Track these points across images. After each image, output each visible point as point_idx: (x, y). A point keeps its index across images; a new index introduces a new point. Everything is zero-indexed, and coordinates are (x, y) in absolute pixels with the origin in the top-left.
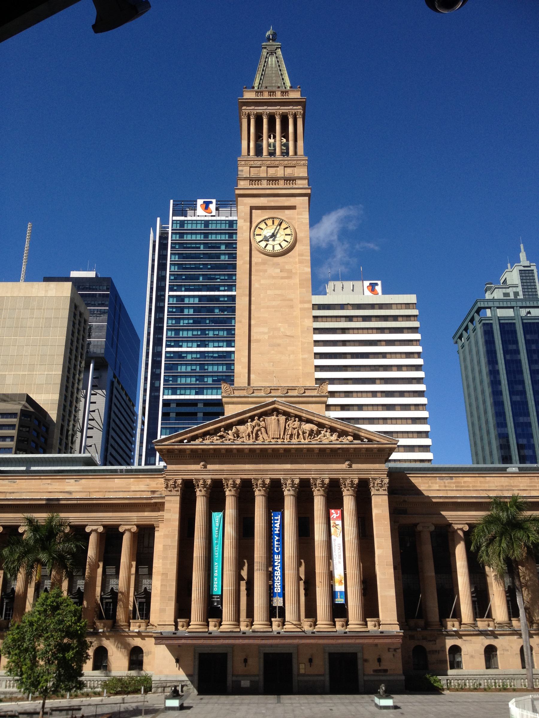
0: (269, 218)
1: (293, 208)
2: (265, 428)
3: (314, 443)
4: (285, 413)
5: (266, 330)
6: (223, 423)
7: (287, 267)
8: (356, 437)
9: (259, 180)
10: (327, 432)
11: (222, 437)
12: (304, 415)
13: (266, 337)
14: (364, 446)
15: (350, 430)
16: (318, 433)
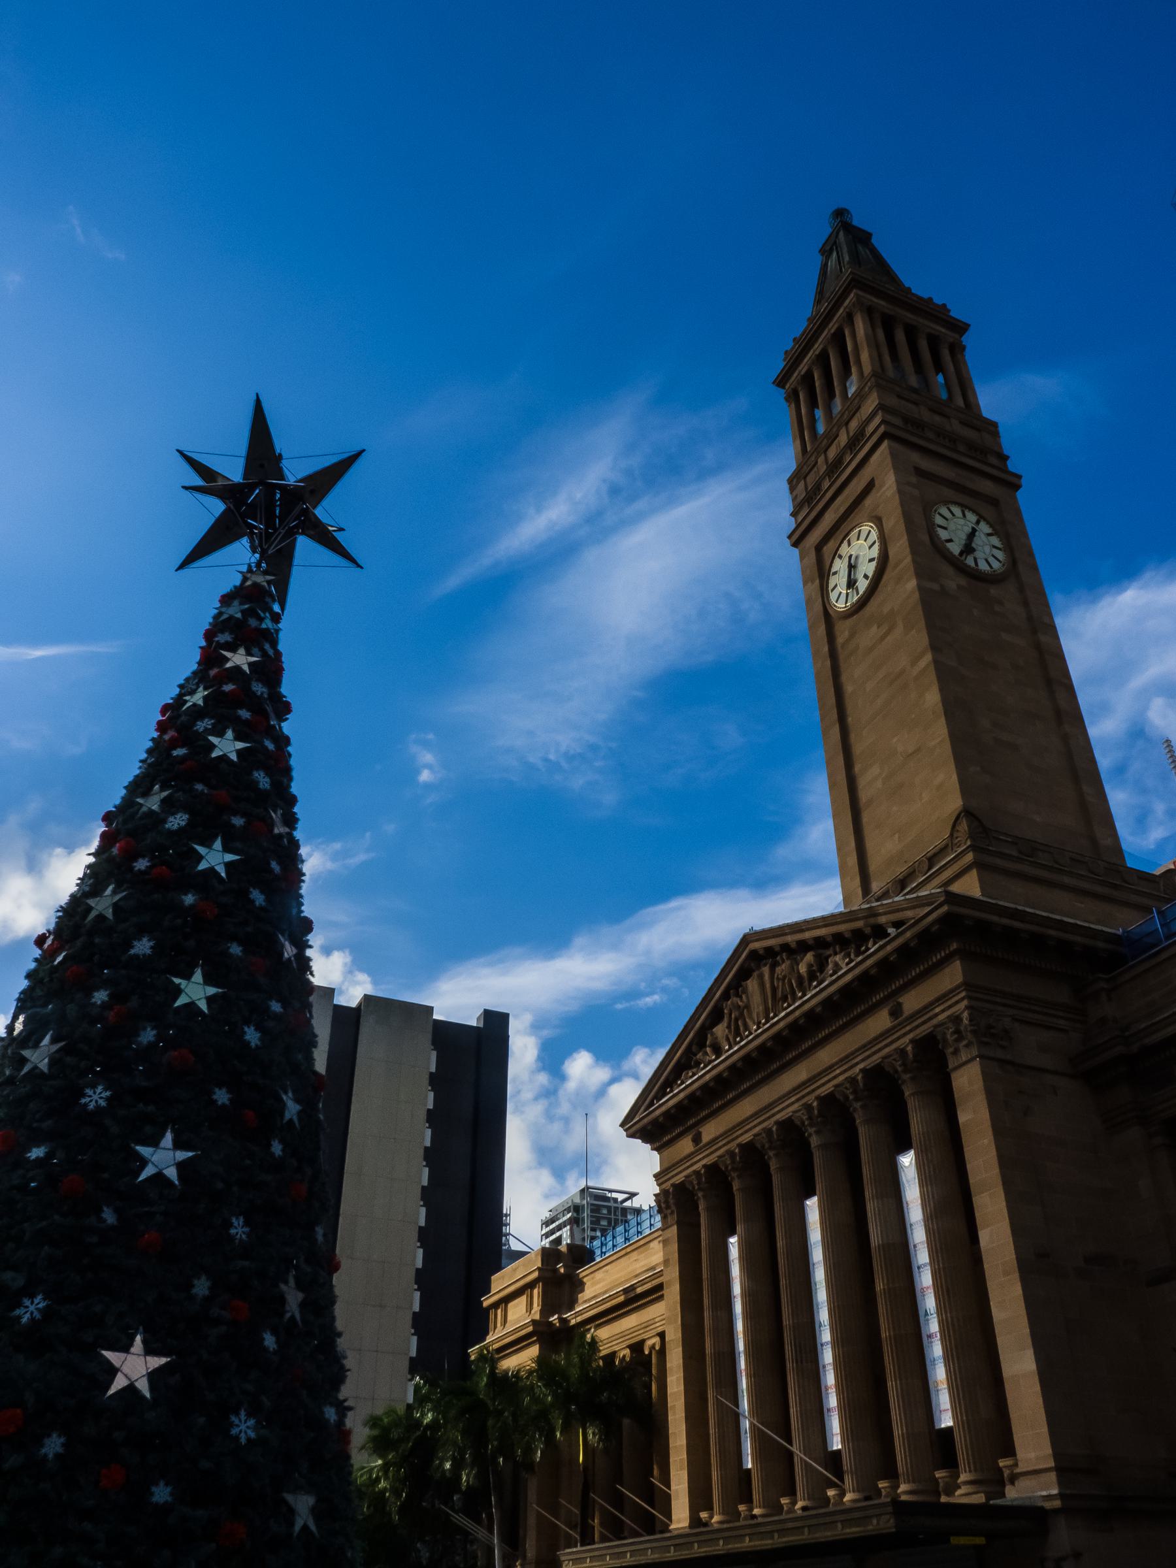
0: (842, 542)
1: (870, 486)
2: (747, 1007)
3: (811, 998)
4: (770, 952)
5: (875, 770)
6: (692, 1035)
7: (886, 610)
8: (879, 932)
9: (818, 486)
10: (836, 954)
11: (698, 1064)
12: (789, 939)
13: (879, 784)
14: (889, 948)
15: (859, 924)
16: (822, 963)
